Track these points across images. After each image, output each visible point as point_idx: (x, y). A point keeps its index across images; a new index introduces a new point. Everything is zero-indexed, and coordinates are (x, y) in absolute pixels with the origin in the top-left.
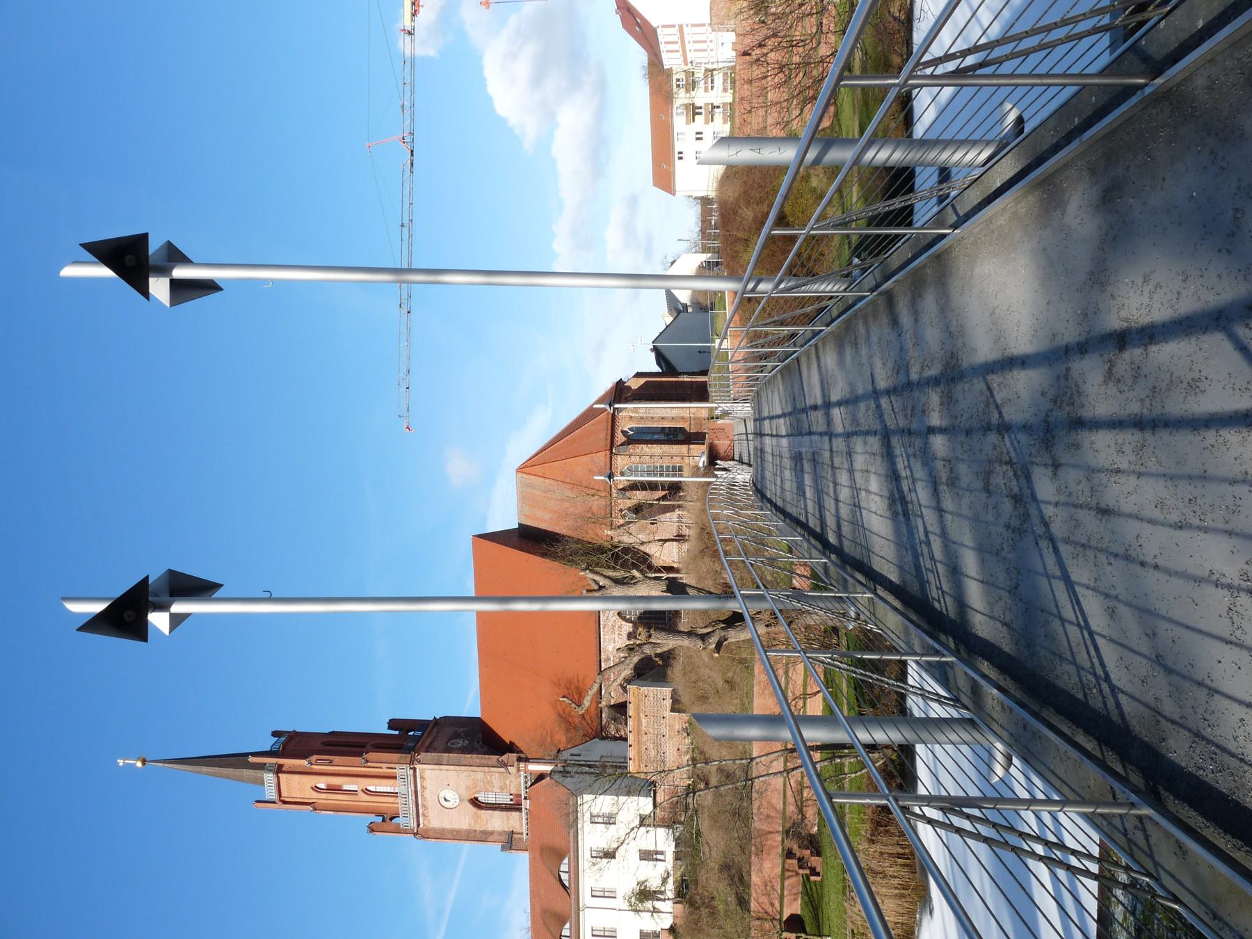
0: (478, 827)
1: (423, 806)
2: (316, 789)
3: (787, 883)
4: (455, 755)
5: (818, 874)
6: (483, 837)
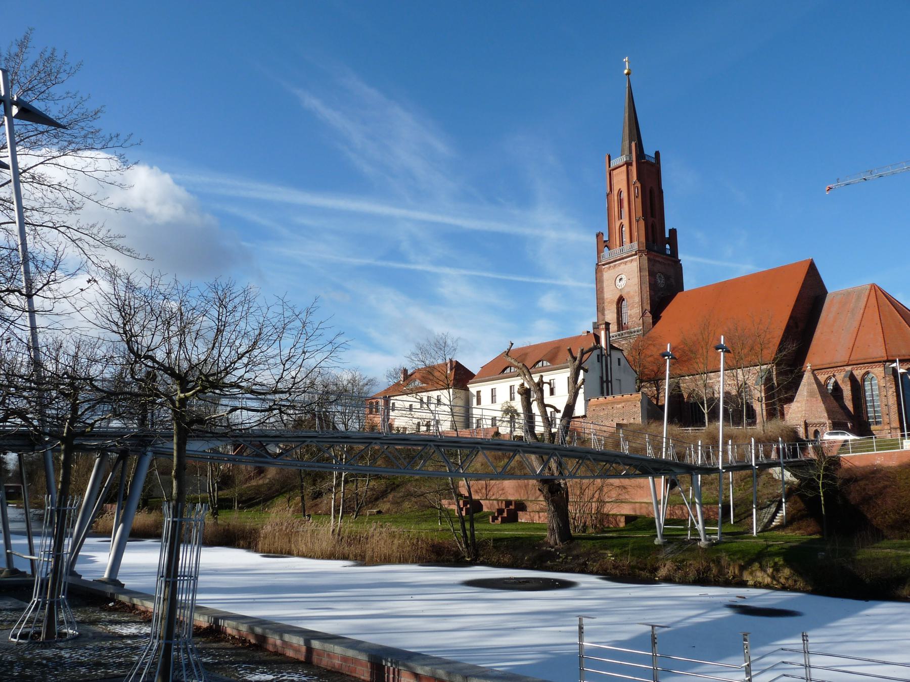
0: (606, 304)
1: (615, 265)
2: (620, 192)
3: (495, 502)
4: (648, 280)
5: (493, 521)
6: (601, 310)
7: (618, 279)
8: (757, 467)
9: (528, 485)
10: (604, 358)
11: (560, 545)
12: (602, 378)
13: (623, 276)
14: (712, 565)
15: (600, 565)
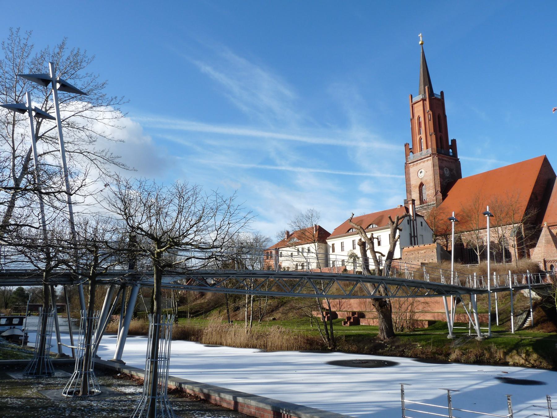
0: (412, 188)
1: (417, 163)
2: (419, 118)
3: (346, 313)
4: (438, 172)
5: (344, 324)
6: (409, 191)
7: (419, 172)
8: (513, 289)
9: (366, 301)
10: (412, 221)
11: (387, 340)
12: (411, 234)
13: (423, 170)
14: (485, 352)
15: (413, 352)
